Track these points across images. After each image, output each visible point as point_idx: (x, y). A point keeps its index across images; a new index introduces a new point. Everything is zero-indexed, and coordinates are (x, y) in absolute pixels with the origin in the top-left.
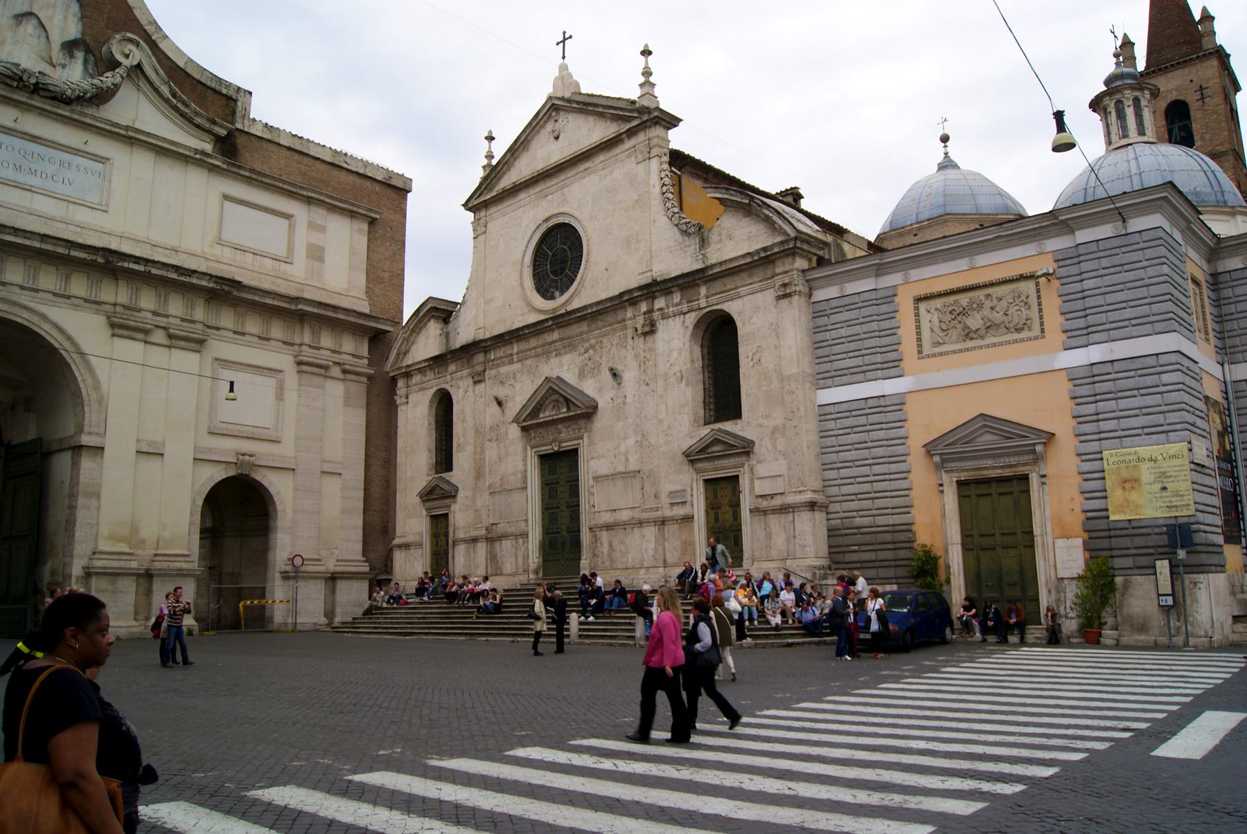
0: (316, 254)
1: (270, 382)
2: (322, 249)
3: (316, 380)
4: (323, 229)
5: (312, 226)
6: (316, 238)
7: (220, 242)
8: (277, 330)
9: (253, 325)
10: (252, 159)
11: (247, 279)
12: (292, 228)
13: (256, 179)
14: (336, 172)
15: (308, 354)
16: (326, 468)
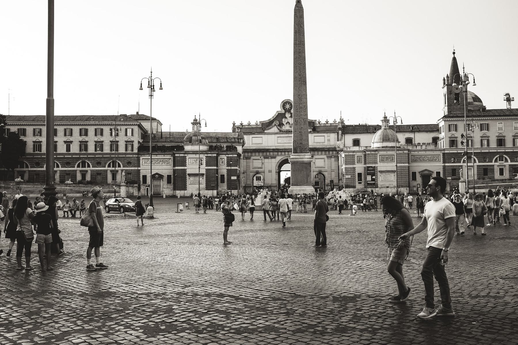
0: (329, 140)
1: (323, 160)
2: (330, 139)
3: (329, 159)
4: (329, 136)
5: (328, 136)
6: (329, 138)
7: (314, 142)
8: (323, 153)
9: (320, 153)
10: (317, 130)
11: (318, 147)
12: (325, 137)
13: (318, 132)
14: (331, 127)
15: (328, 155)
16: (332, 170)
